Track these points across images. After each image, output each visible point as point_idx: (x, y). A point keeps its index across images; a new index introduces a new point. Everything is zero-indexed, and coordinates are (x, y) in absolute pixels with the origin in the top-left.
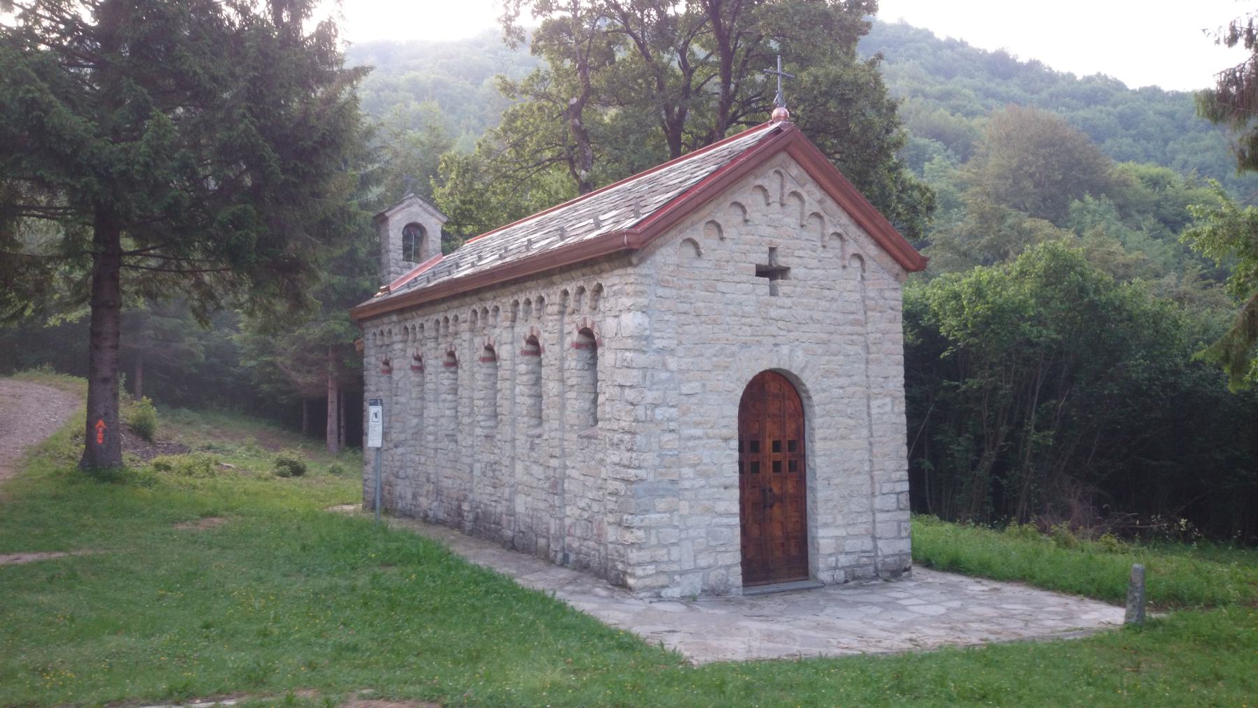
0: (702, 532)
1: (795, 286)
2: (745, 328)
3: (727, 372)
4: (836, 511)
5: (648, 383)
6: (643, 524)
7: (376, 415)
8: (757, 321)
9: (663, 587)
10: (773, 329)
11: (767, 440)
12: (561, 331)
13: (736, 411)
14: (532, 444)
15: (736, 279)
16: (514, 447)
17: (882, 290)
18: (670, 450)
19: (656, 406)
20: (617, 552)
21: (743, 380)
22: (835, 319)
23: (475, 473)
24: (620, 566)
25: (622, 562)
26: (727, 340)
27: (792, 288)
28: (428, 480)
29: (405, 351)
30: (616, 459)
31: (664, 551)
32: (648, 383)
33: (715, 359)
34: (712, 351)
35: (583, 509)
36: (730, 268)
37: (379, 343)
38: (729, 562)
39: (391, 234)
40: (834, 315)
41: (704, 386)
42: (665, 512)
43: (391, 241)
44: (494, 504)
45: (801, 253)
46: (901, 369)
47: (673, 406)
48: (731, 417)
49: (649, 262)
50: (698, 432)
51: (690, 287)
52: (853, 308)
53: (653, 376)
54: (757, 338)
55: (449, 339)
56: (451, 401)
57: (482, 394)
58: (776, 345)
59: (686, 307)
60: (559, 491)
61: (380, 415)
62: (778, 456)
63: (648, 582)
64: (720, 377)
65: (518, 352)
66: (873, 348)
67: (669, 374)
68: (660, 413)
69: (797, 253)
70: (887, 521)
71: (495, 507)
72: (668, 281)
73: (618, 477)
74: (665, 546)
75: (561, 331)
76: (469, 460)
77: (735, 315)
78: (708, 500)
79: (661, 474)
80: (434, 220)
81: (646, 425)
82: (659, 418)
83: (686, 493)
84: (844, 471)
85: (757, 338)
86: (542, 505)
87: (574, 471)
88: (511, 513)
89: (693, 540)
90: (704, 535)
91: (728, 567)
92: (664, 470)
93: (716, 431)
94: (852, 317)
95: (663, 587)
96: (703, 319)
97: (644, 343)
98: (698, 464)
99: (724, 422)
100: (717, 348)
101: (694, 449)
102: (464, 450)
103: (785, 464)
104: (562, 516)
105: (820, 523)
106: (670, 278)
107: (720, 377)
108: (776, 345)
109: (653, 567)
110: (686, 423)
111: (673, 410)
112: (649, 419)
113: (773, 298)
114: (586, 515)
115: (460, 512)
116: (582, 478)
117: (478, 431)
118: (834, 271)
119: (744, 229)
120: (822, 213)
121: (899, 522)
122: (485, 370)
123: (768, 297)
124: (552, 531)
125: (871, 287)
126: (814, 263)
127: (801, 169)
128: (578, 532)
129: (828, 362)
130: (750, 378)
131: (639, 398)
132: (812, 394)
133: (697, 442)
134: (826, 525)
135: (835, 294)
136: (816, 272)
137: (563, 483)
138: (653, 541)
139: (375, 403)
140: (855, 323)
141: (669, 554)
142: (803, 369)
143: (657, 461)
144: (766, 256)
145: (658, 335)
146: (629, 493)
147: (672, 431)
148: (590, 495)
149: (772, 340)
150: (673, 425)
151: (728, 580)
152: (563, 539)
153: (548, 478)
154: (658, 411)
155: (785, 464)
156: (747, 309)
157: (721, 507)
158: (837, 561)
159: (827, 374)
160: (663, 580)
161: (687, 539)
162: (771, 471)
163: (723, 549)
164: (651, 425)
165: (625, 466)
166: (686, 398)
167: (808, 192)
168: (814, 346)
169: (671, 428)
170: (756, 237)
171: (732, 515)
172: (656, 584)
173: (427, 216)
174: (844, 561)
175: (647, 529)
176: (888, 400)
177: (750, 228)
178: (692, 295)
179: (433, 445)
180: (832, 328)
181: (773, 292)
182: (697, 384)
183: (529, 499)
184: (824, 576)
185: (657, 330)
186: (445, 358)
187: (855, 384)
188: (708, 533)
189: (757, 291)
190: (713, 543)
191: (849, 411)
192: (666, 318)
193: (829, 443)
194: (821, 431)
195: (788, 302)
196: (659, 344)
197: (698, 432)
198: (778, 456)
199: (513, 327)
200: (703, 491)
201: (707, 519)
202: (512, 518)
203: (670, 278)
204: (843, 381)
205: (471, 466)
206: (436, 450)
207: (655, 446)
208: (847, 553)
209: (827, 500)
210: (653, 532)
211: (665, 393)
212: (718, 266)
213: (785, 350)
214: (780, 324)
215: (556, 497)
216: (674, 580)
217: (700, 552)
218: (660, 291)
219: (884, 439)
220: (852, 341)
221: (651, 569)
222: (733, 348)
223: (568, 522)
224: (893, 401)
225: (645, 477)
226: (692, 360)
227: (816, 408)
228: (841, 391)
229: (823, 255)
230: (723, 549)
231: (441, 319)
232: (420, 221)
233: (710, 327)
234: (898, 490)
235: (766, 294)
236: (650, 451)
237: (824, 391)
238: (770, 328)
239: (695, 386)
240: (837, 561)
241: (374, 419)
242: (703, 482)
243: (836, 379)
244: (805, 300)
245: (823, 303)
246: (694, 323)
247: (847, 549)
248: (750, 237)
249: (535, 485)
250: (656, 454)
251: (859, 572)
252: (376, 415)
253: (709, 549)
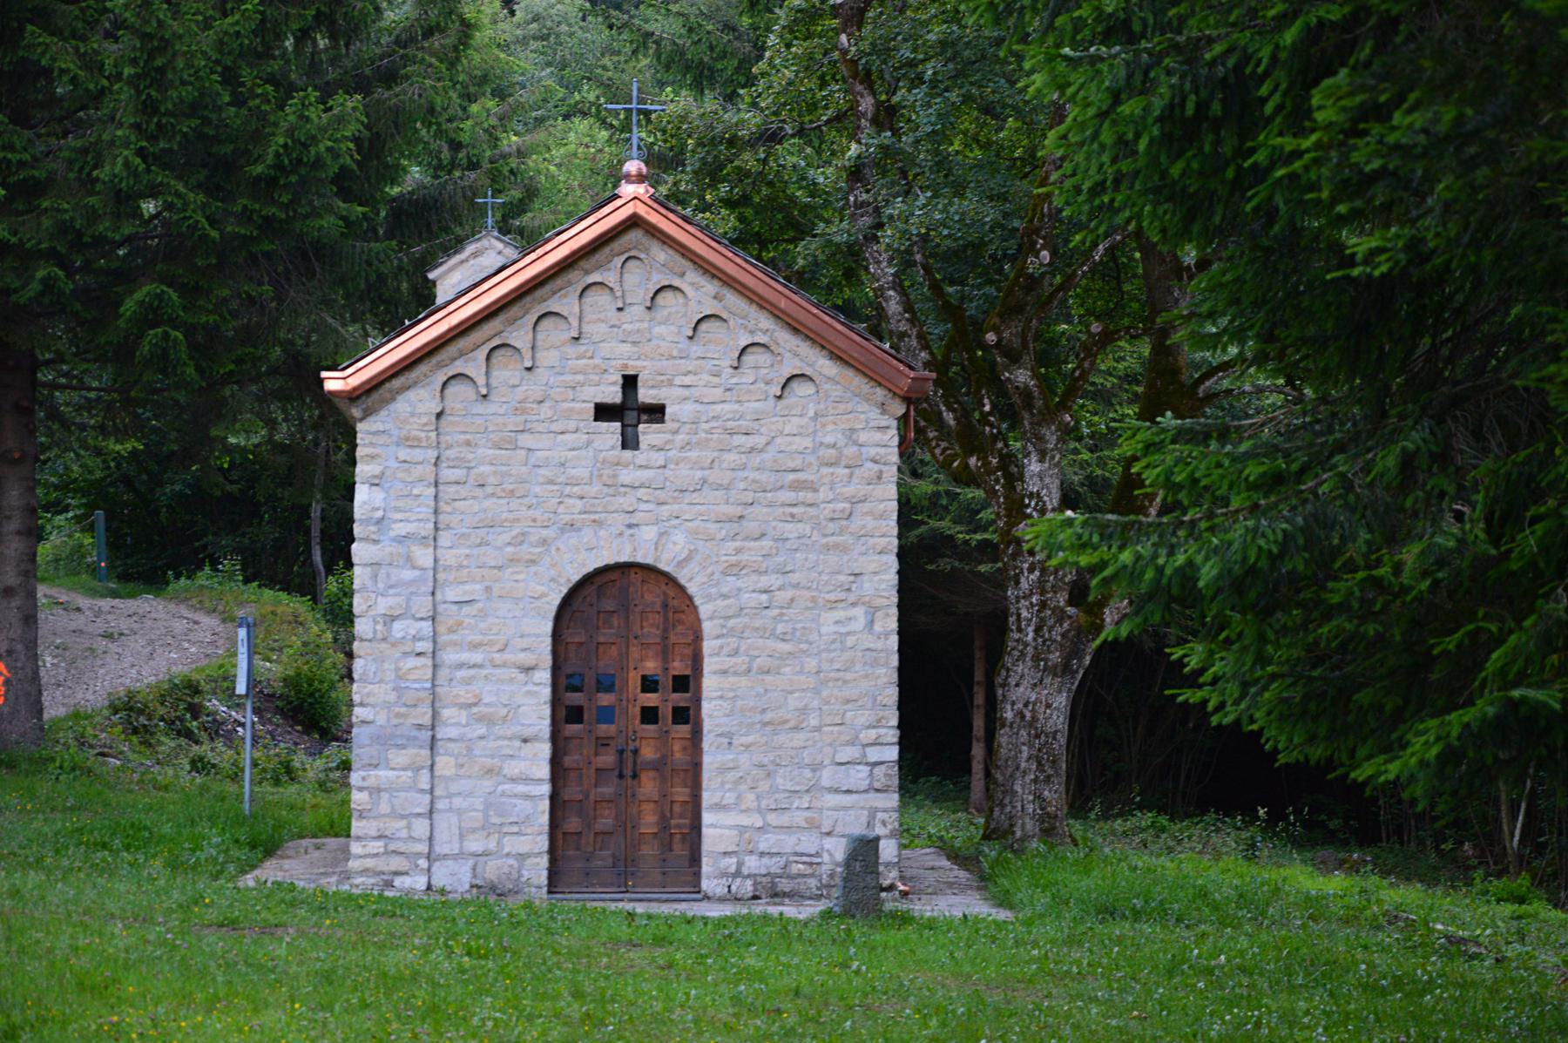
2: (570, 501)
3: (533, 569)
4: (743, 787)
6: (365, 784)
9: (397, 873)
10: (627, 502)
11: (632, 674)
15: (555, 427)
17: (853, 430)
18: (415, 681)
19: (394, 618)
21: (562, 580)
22: (754, 481)
26: (534, 520)
27: (668, 436)
31: (403, 823)
32: (381, 585)
33: (510, 549)
34: (506, 538)
36: (545, 411)
38: (524, 849)
40: (753, 475)
41: (488, 589)
42: (404, 769)
45: (687, 380)
46: (892, 563)
48: (538, 636)
49: (383, 413)
50: (477, 657)
51: (468, 443)
52: (797, 462)
53: (388, 575)
54: (593, 517)
58: (630, 526)
62: (651, 699)
63: (369, 863)
64: (520, 577)
67: (417, 573)
68: (398, 628)
69: (678, 381)
70: (845, 808)
72: (419, 440)
74: (403, 817)
77: (551, 482)
78: (492, 757)
79: (398, 715)
81: (374, 645)
82: (400, 635)
83: (452, 745)
84: (765, 724)
89: (460, 812)
91: (522, 857)
92: (403, 710)
93: (507, 656)
94: (792, 476)
95: (397, 873)
96: (489, 490)
97: (373, 528)
98: (475, 704)
99: (525, 643)
100: (514, 533)
101: (468, 681)
106: (423, 435)
107: (520, 577)
108: (630, 526)
109: (381, 843)
110: (455, 644)
112: (379, 636)
113: (628, 454)
118: (757, 405)
119: (572, 350)
120: (724, 315)
121: (873, 812)
125: (830, 427)
127: (671, 252)
129: (738, 551)
132: (697, 601)
133: (472, 672)
134: (720, 807)
135: (759, 440)
136: (718, 408)
138: (384, 808)
141: (409, 827)
143: (392, 697)
145: (398, 516)
151: (520, 876)
154: (397, 625)
156: (574, 472)
157: (514, 768)
158: (740, 864)
159: (734, 569)
160: (396, 863)
161: (450, 810)
163: (515, 829)
164: (383, 646)
166: (455, 607)
167: (692, 284)
169: (418, 650)
170: (597, 361)
172: (385, 869)
174: (752, 864)
175: (376, 791)
176: (859, 612)
177: (583, 348)
178: (470, 456)
180: (749, 497)
182: (477, 587)
184: (706, 885)
185: (397, 510)
187: (797, 586)
188: (488, 806)
189: (595, 444)
190: (494, 820)
191: (780, 628)
192: (415, 491)
193: (731, 679)
194: (715, 659)
195: (658, 458)
196: (401, 529)
197: (477, 657)
198: (651, 699)
200: (483, 743)
201: (487, 784)
204: (773, 580)
207: (390, 676)
208: (762, 854)
209: (723, 770)
210: (385, 796)
211: (409, 600)
212: (519, 410)
213: (649, 533)
214: (641, 493)
216: (417, 866)
217: (474, 831)
219: (848, 676)
220: (793, 516)
221: (376, 847)
222: (545, 532)
225: (370, 718)
228: (764, 597)
229: (734, 380)
230: (515, 829)
233: (504, 501)
234: (873, 759)
235: (613, 448)
237: (725, 596)
238: (621, 500)
239: (475, 590)
240: (740, 864)
242: (482, 731)
243: (754, 577)
244: (693, 454)
246: (474, 498)
247: (763, 847)
248: (584, 361)
250: (390, 686)
251: (784, 885)
253: (486, 828)
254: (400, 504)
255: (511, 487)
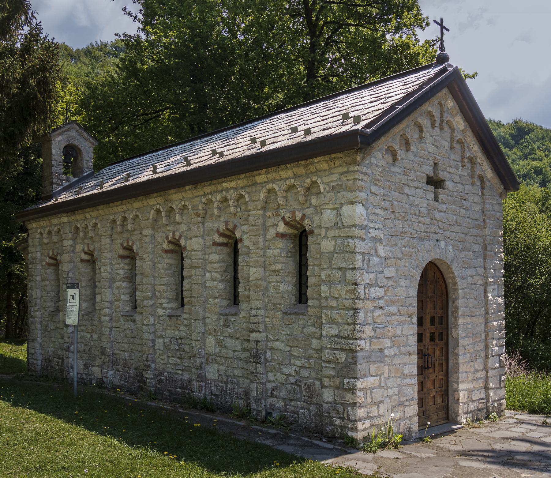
0: (396, 391)
1: (448, 195)
5: (365, 266)
7: (73, 297)
8: (428, 220)
12: (264, 225)
13: (414, 292)
14: (227, 321)
15: (415, 184)
16: (205, 324)
20: (334, 409)
23: (157, 347)
24: (338, 422)
25: (340, 418)
28: (103, 353)
29: (74, 247)
30: (334, 331)
32: (365, 266)
35: (289, 375)
37: (45, 241)
39: (54, 152)
43: (54, 157)
44: (180, 372)
47: (381, 287)
52: (477, 216)
53: (369, 260)
54: (427, 234)
55: (126, 235)
56: (126, 288)
57: (166, 281)
59: (387, 204)
60: (262, 360)
61: (77, 297)
65: (209, 243)
66: (489, 248)
71: (182, 375)
73: (338, 346)
75: (264, 225)
76: (151, 337)
80: (87, 144)
81: (365, 302)
82: (373, 296)
85: (427, 234)
86: (239, 373)
87: (277, 343)
88: (201, 378)
89: (390, 397)
90: (397, 393)
91: (411, 417)
94: (477, 222)
102: (145, 327)
103: (437, 335)
104: (264, 381)
105: (460, 380)
107: (407, 264)
111: (382, 290)
114: (293, 380)
115: (141, 379)
116: (288, 349)
117: (160, 312)
122: (167, 261)
123: (432, 202)
124: (254, 394)
126: (457, 179)
128: (283, 394)
130: (424, 266)
131: (361, 279)
132: (458, 280)
134: (463, 382)
137: (265, 353)
139: (72, 287)
140: (478, 227)
142: (452, 261)
144: (432, 168)
146: (350, 360)
147: (381, 308)
148: (298, 363)
149: (435, 237)
150: (382, 303)
151: (411, 428)
152: (265, 400)
153: (245, 350)
155: (437, 335)
162: (429, 340)
165: (344, 338)
168: (457, 243)
171: (411, 376)
173: (82, 140)
179: (109, 324)
181: (436, 199)
183: (223, 368)
186: (122, 252)
190: (402, 399)
192: (377, 211)
196: (373, 233)
199: (203, 223)
202: (203, 384)
203: (379, 178)
205: (153, 341)
206: (111, 328)
207: (370, 321)
211: (376, 275)
215: (259, 366)
218: (374, 189)
223: (270, 386)
224: (498, 287)
226: (390, 249)
227: (460, 291)
231: (119, 219)
232: (76, 143)
233: (400, 222)
236: (367, 324)
241: (72, 300)
245: (462, 210)
249: (231, 356)
252: (73, 297)
254: (371, 217)
255: (404, 214)
